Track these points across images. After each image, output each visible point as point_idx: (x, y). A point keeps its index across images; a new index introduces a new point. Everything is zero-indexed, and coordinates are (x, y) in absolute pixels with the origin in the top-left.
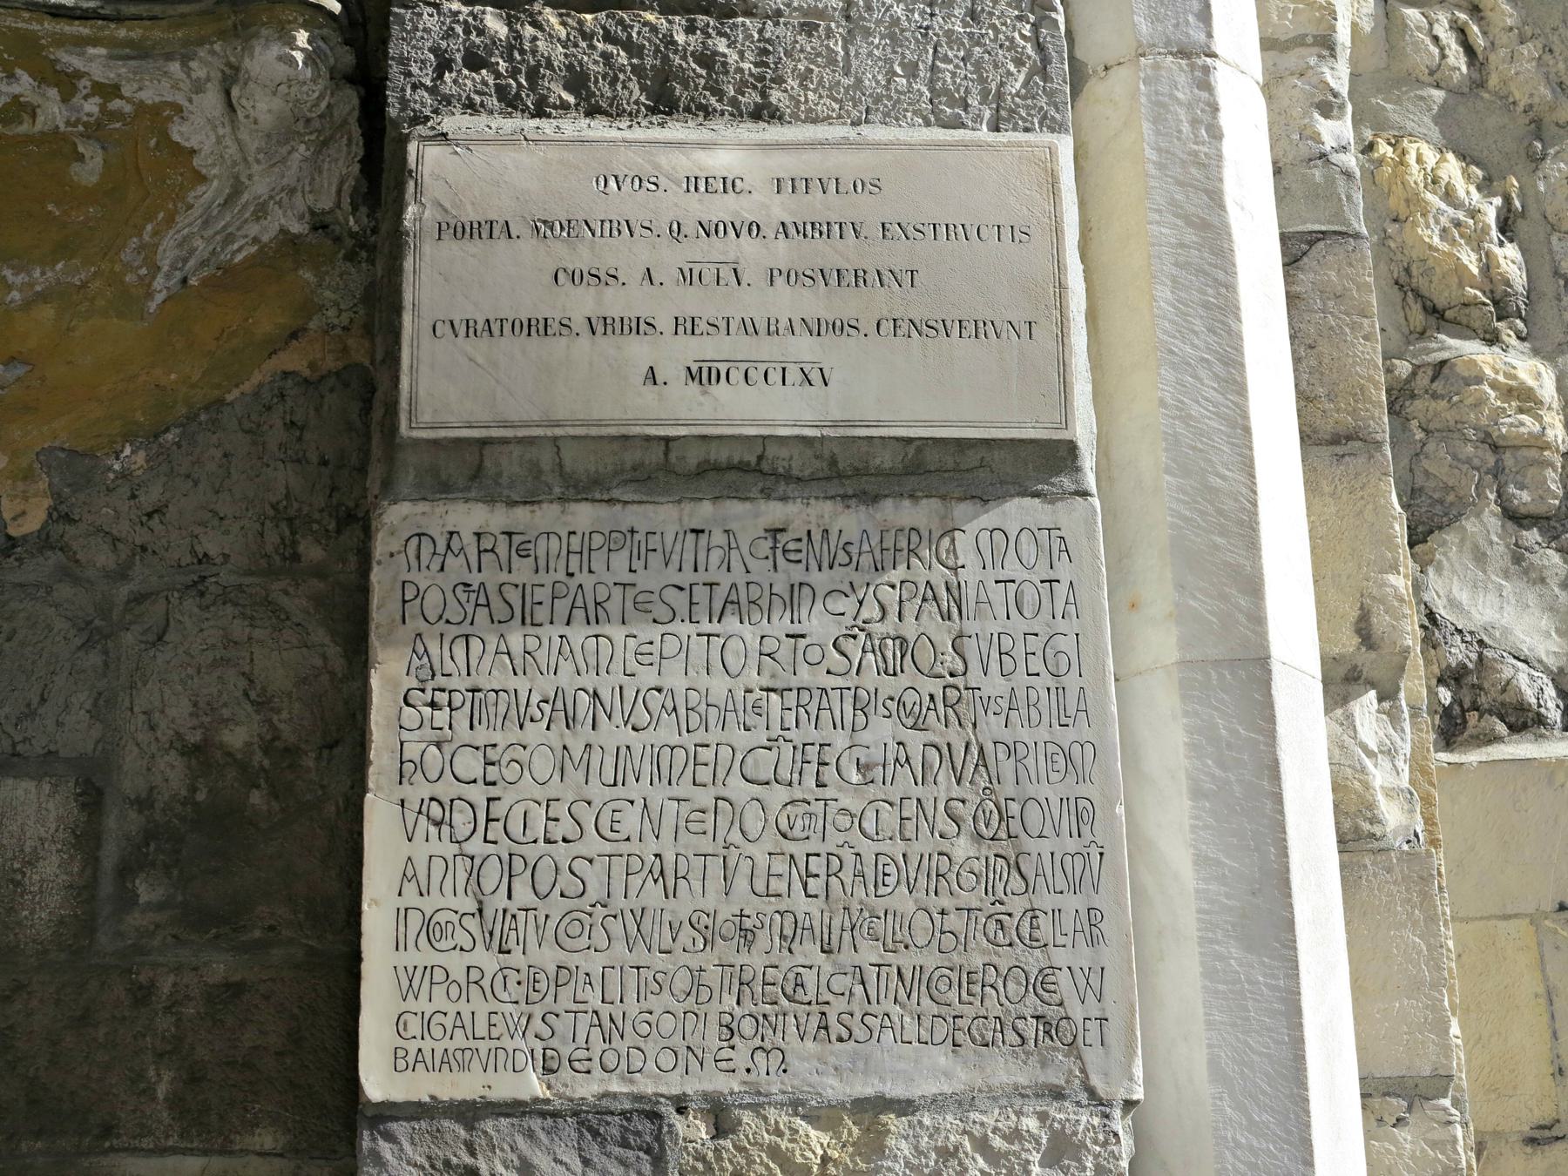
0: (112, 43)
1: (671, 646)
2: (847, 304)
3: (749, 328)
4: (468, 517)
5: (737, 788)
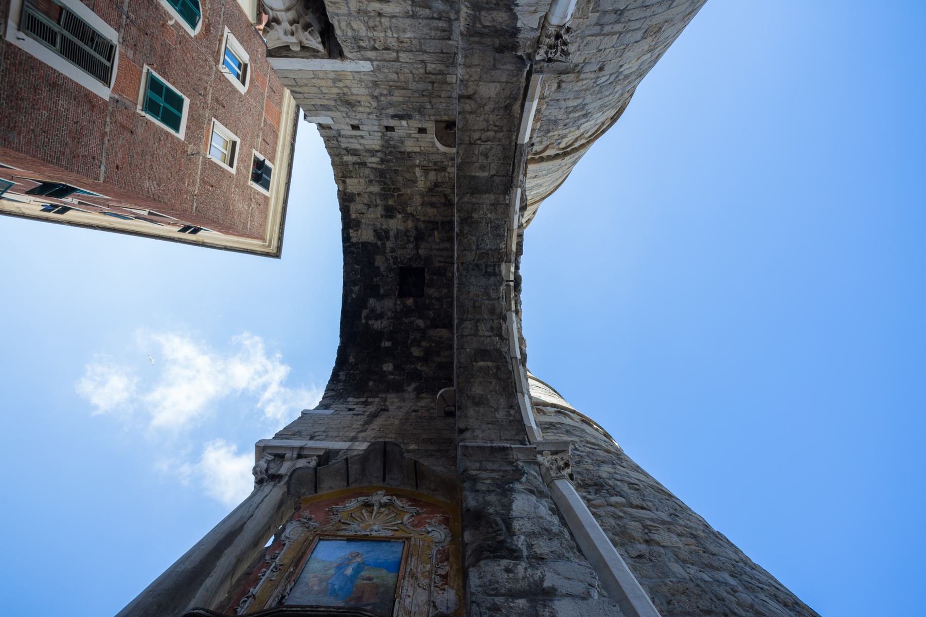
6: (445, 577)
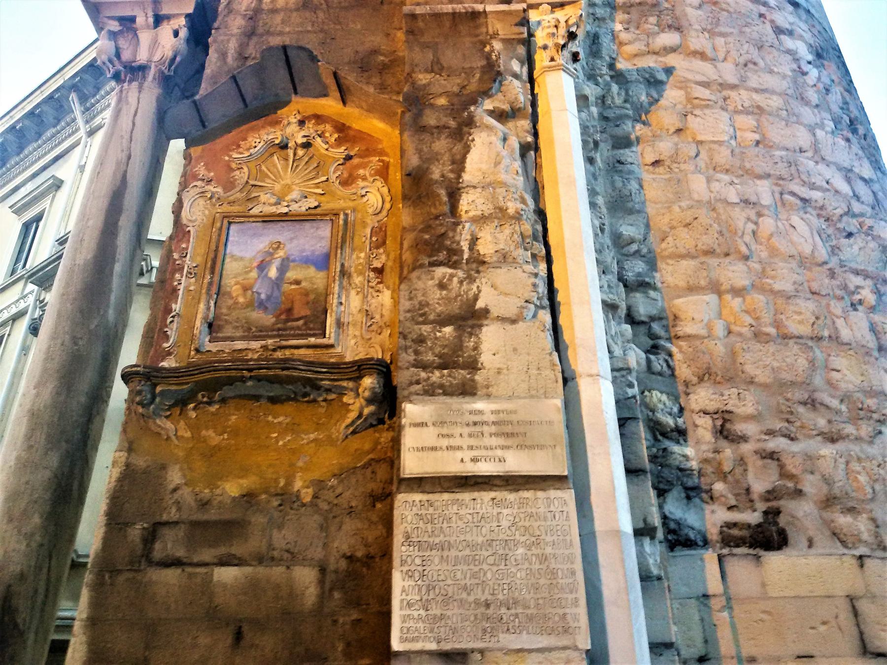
1: (468, 529)
2: (509, 442)
3: (486, 448)
4: (418, 497)
5: (485, 567)
6: (380, 271)
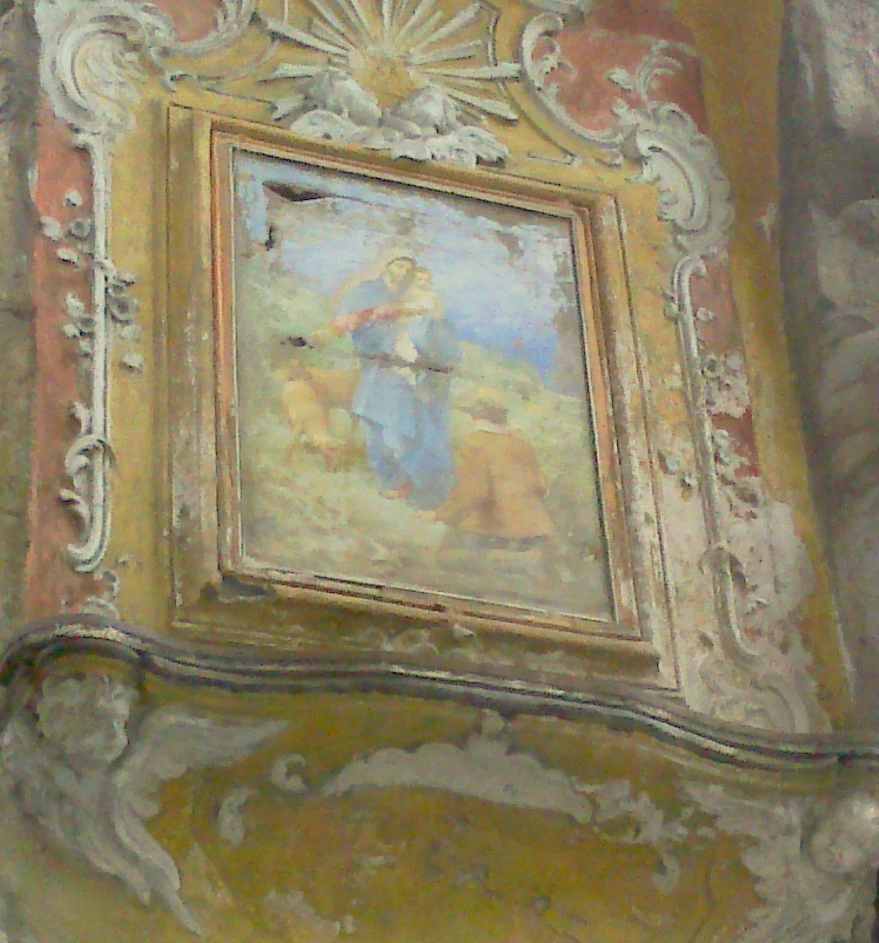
0: (732, 786)
